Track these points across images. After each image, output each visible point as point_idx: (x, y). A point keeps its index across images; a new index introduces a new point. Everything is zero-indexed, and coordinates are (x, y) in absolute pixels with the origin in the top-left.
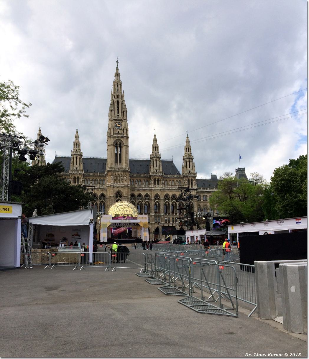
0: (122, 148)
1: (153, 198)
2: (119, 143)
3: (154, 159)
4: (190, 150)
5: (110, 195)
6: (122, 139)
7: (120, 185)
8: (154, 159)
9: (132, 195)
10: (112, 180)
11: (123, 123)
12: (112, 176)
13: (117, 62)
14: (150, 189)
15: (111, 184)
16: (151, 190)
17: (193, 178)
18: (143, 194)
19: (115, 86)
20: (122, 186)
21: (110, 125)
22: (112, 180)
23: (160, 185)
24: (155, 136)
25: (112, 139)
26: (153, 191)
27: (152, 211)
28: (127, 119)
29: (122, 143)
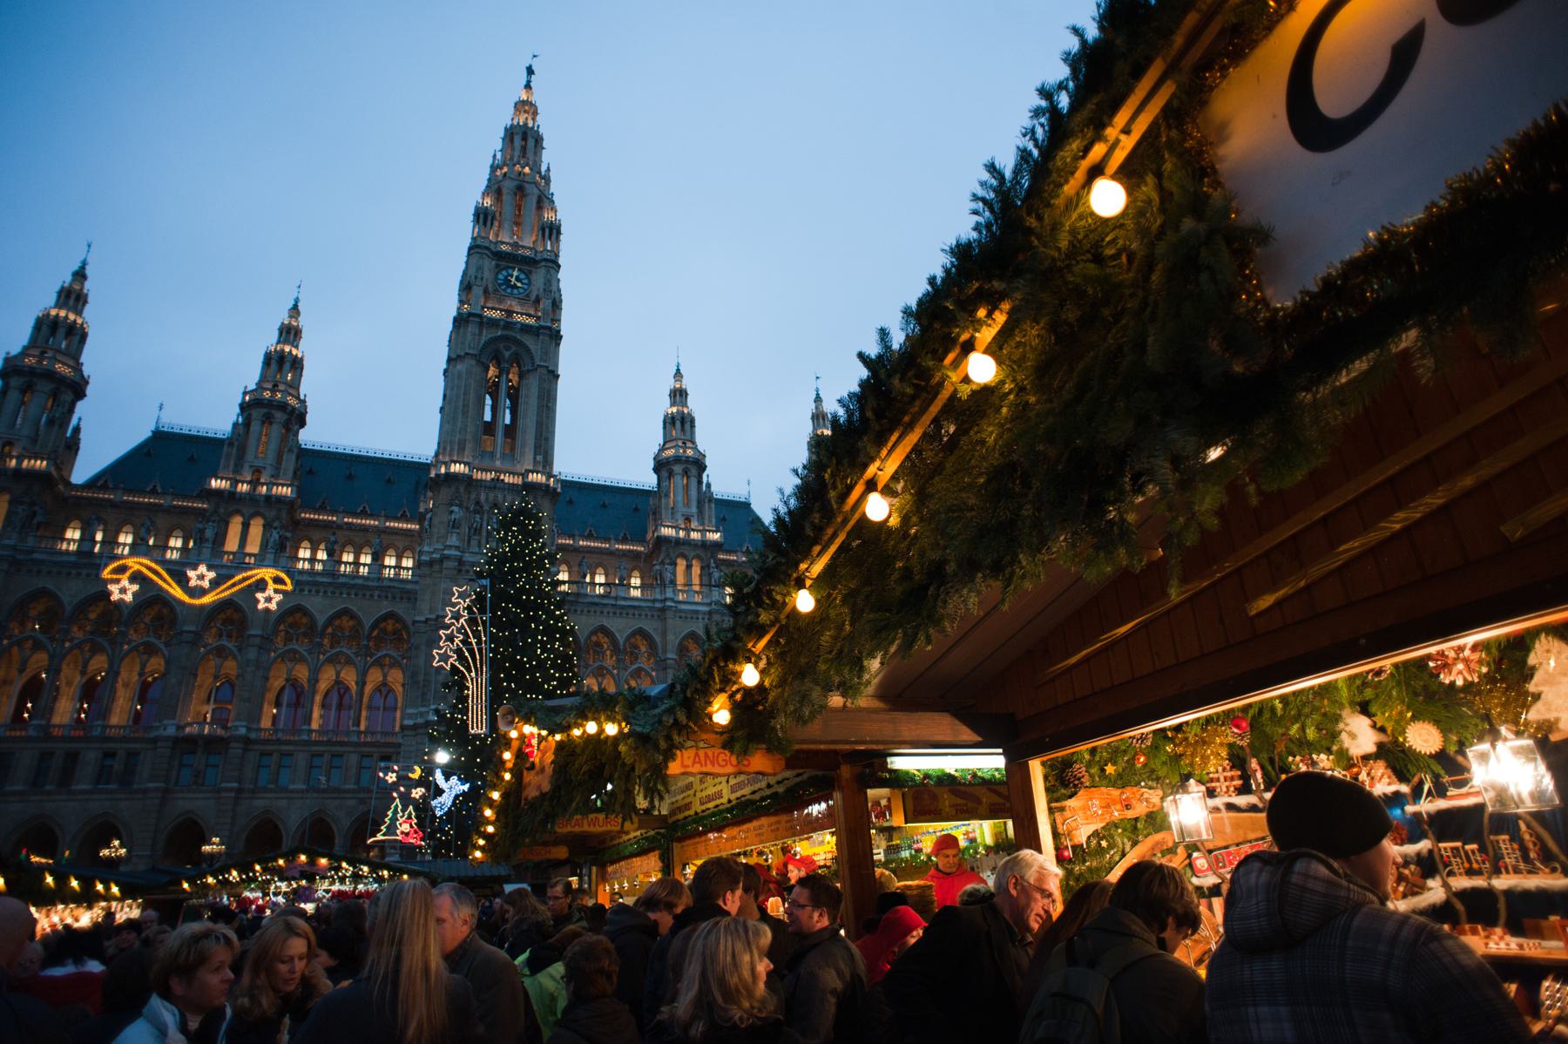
5: (431, 611)
6: (529, 341)
10: (455, 525)
11: (538, 278)
12: (455, 509)
13: (530, 71)
14: (658, 605)
15: (450, 547)
16: (663, 610)
18: (621, 627)
19: (512, 140)
21: (472, 272)
22: (455, 525)
24: (678, 374)
26: (669, 614)
28: (561, 261)
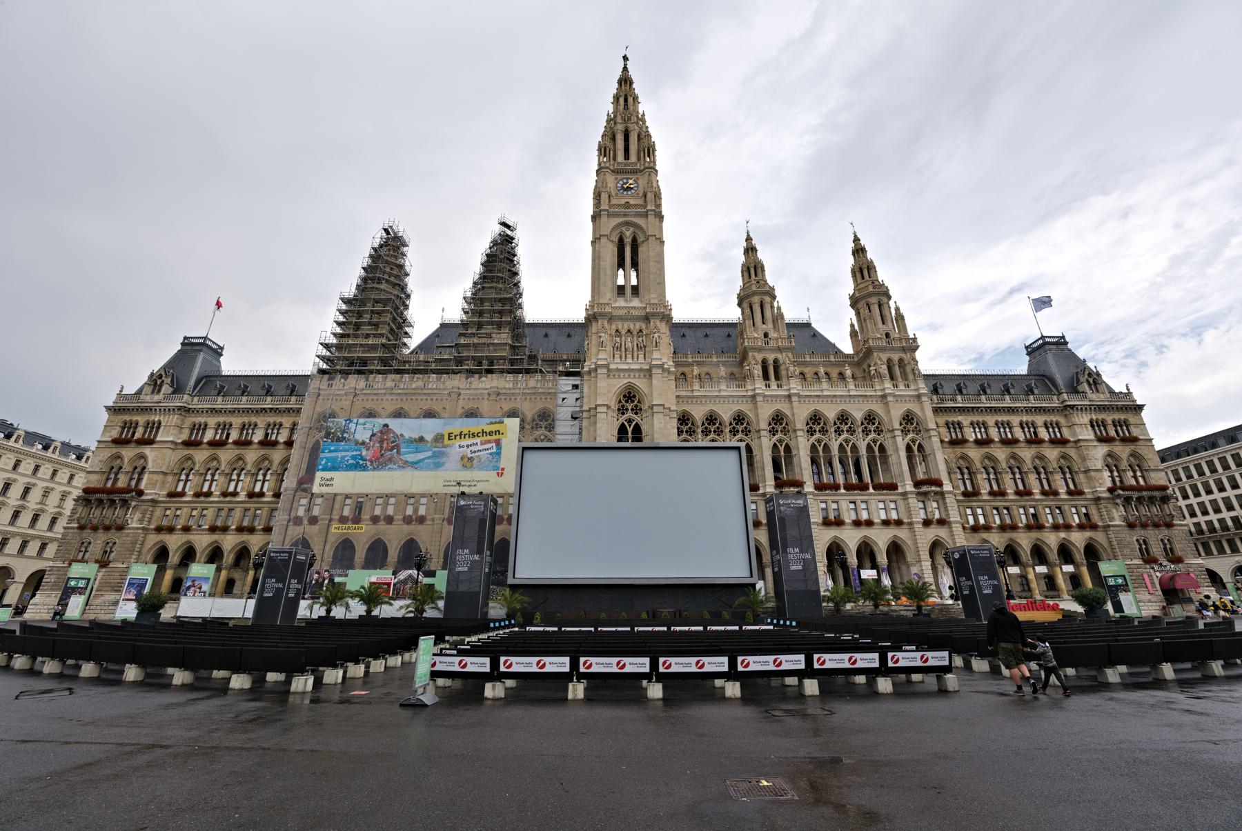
0: (641, 249)
1: (763, 425)
2: (628, 233)
3: (756, 300)
4: (872, 272)
7: (633, 367)
8: (756, 300)
9: (684, 419)
13: (625, 58)
17: (903, 356)
20: (641, 370)
23: (784, 380)
25: (604, 219)
27: (764, 476)
29: (641, 238)
